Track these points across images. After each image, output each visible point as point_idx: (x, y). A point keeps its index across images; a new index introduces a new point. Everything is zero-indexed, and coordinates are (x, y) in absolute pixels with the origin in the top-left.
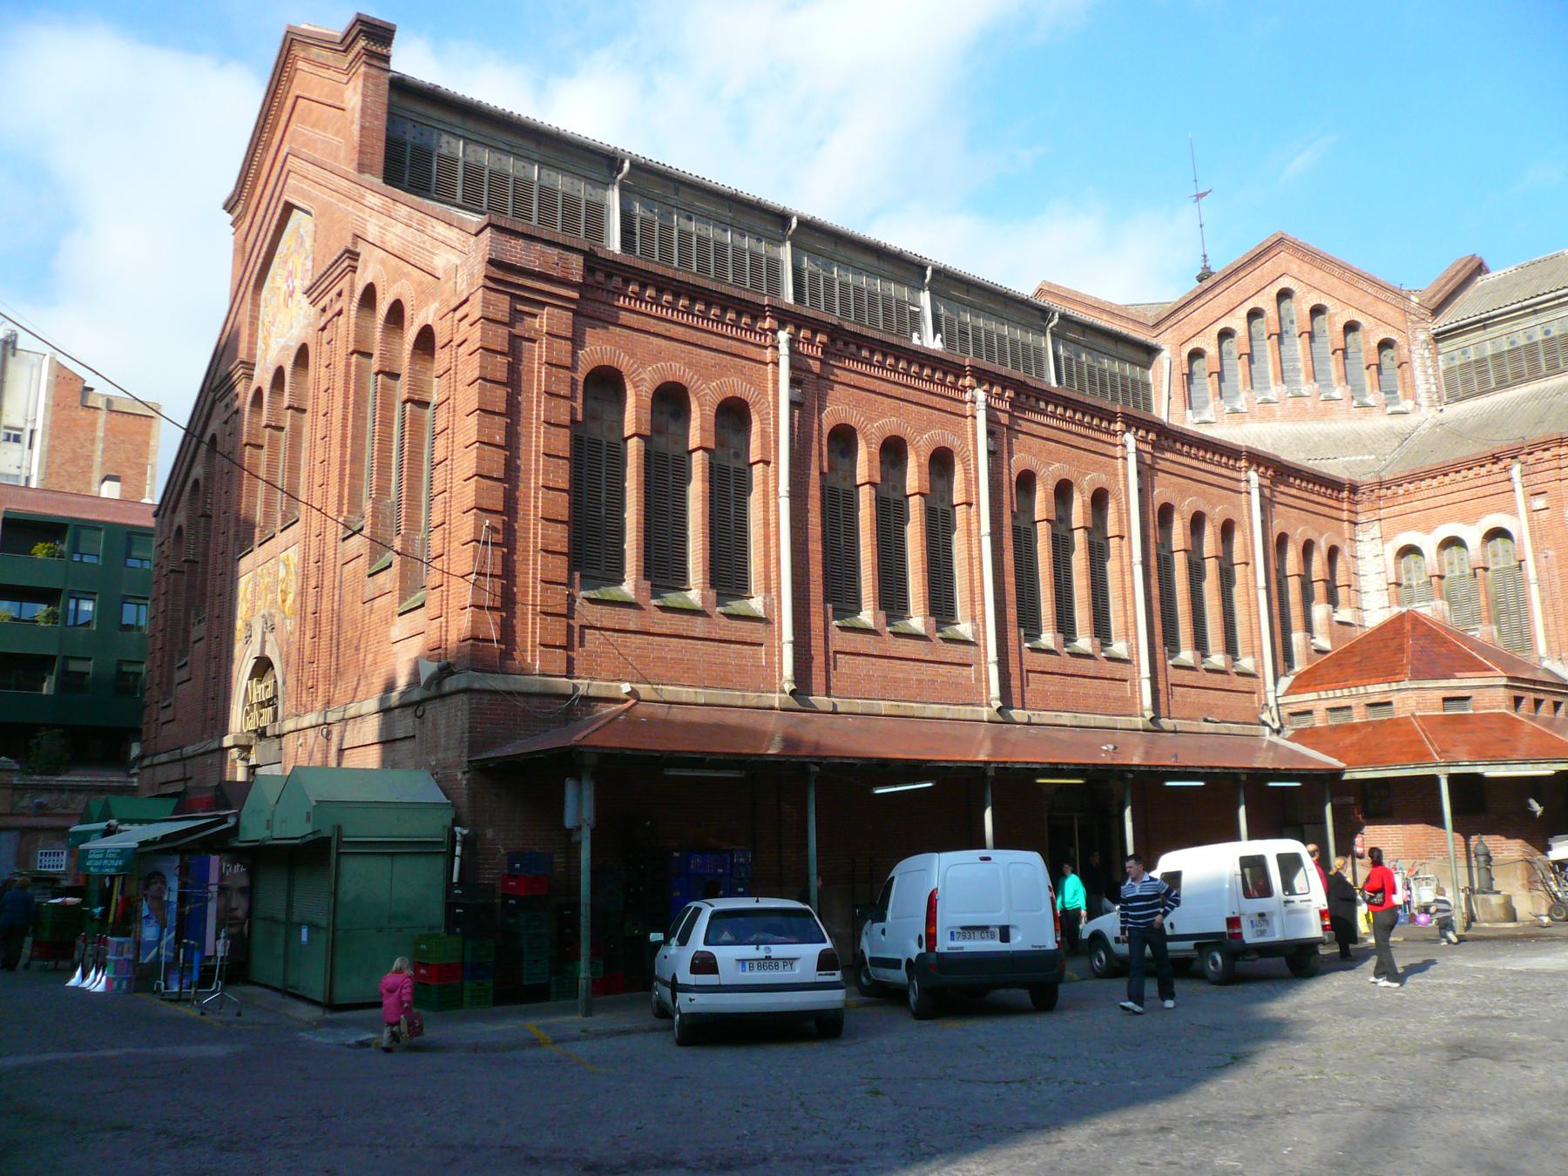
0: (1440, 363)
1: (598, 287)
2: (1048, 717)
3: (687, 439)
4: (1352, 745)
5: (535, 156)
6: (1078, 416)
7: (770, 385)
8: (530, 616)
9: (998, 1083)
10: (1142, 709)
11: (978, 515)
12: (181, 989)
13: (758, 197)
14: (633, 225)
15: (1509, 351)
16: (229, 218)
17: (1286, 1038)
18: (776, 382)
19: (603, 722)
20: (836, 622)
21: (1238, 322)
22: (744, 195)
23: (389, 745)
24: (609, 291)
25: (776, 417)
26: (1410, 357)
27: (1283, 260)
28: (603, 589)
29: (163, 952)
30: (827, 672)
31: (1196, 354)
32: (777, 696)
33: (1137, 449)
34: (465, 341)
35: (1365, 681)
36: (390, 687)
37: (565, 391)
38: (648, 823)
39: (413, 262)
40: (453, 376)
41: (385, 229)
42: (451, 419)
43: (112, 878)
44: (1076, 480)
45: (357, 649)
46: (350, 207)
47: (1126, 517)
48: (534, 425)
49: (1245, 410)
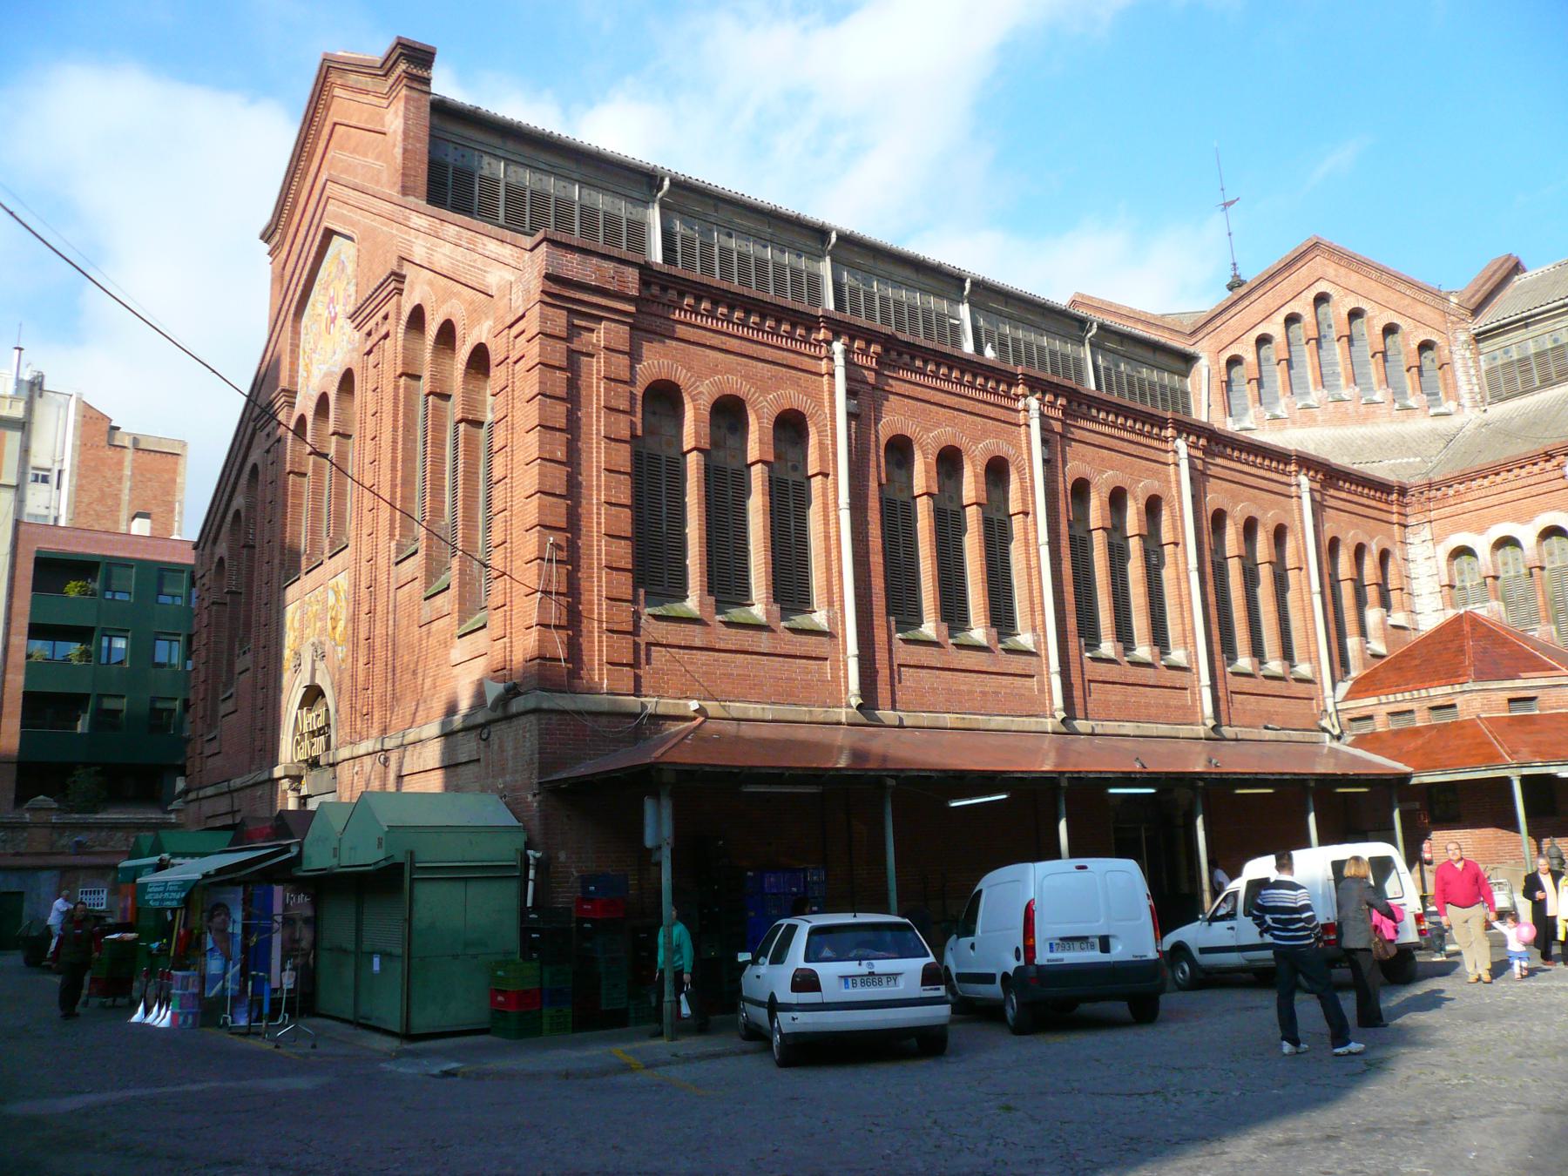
0: (1482, 363)
1: (654, 300)
2: (1111, 727)
3: (745, 451)
4: (1416, 750)
5: (575, 176)
6: (1130, 423)
7: (826, 396)
8: (596, 634)
9: (1130, 1095)
10: (1203, 718)
11: (1036, 524)
12: (250, 1023)
13: (797, 212)
14: (674, 243)
15: (1552, 349)
16: (267, 248)
17: (1413, 1043)
18: (832, 394)
19: (675, 741)
20: (899, 635)
21: (1275, 328)
22: (783, 210)
23: (452, 769)
24: (664, 305)
25: (834, 428)
26: (1451, 358)
27: (1319, 264)
28: (667, 606)
29: (229, 985)
30: (892, 685)
31: (1234, 361)
32: (844, 710)
33: (1189, 455)
34: (523, 357)
35: (1427, 685)
36: (451, 710)
37: (623, 405)
38: (721, 842)
39: (463, 281)
40: (510, 394)
41: (432, 250)
42: (509, 436)
43: (174, 911)
44: (1130, 487)
45: (415, 673)
46: (394, 229)
47: (1180, 523)
48: (595, 441)
49: (1286, 416)
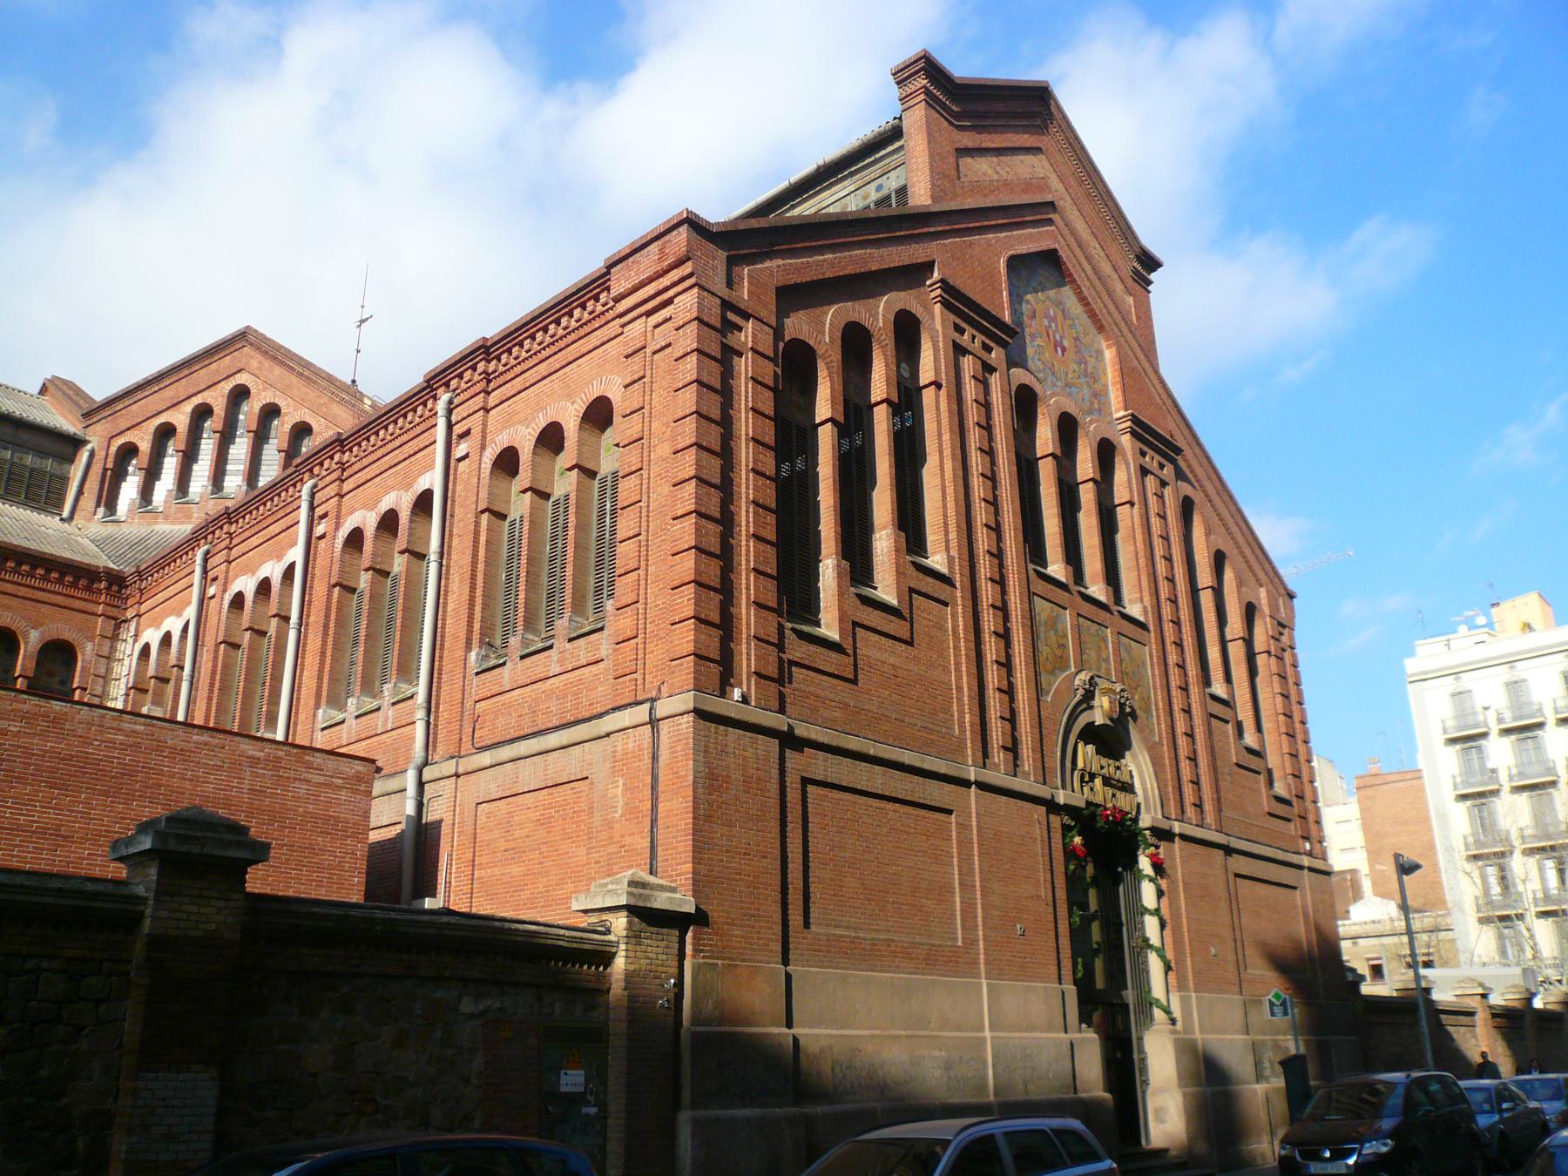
21: (181, 419)
31: (129, 451)
